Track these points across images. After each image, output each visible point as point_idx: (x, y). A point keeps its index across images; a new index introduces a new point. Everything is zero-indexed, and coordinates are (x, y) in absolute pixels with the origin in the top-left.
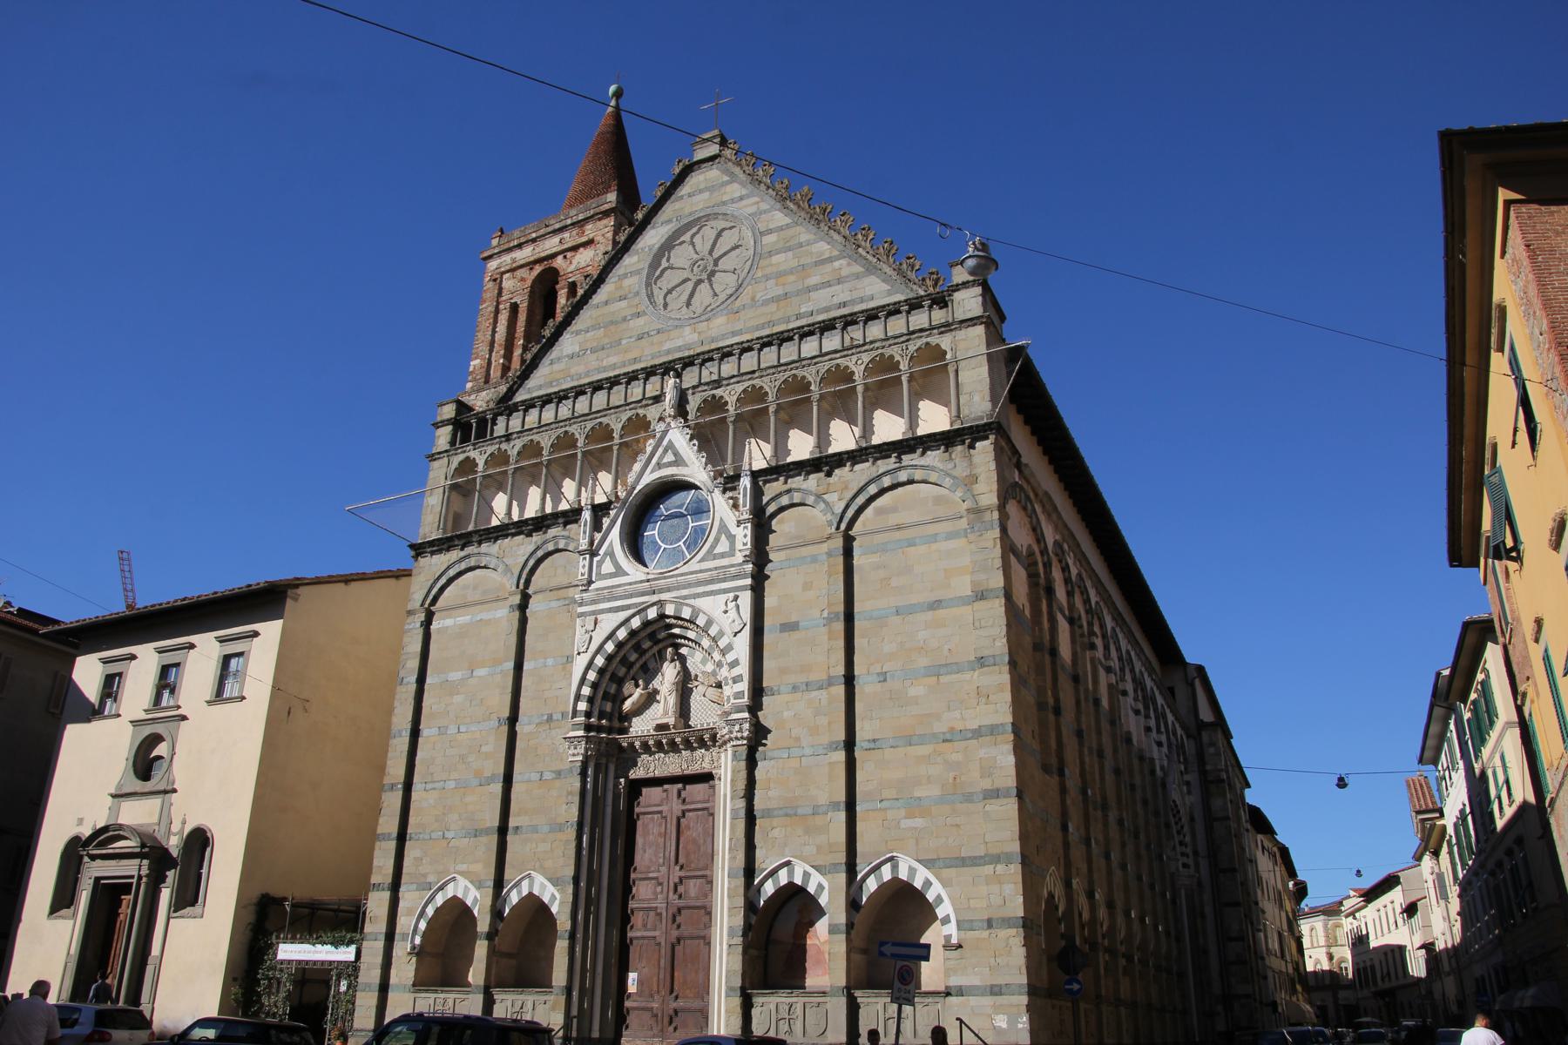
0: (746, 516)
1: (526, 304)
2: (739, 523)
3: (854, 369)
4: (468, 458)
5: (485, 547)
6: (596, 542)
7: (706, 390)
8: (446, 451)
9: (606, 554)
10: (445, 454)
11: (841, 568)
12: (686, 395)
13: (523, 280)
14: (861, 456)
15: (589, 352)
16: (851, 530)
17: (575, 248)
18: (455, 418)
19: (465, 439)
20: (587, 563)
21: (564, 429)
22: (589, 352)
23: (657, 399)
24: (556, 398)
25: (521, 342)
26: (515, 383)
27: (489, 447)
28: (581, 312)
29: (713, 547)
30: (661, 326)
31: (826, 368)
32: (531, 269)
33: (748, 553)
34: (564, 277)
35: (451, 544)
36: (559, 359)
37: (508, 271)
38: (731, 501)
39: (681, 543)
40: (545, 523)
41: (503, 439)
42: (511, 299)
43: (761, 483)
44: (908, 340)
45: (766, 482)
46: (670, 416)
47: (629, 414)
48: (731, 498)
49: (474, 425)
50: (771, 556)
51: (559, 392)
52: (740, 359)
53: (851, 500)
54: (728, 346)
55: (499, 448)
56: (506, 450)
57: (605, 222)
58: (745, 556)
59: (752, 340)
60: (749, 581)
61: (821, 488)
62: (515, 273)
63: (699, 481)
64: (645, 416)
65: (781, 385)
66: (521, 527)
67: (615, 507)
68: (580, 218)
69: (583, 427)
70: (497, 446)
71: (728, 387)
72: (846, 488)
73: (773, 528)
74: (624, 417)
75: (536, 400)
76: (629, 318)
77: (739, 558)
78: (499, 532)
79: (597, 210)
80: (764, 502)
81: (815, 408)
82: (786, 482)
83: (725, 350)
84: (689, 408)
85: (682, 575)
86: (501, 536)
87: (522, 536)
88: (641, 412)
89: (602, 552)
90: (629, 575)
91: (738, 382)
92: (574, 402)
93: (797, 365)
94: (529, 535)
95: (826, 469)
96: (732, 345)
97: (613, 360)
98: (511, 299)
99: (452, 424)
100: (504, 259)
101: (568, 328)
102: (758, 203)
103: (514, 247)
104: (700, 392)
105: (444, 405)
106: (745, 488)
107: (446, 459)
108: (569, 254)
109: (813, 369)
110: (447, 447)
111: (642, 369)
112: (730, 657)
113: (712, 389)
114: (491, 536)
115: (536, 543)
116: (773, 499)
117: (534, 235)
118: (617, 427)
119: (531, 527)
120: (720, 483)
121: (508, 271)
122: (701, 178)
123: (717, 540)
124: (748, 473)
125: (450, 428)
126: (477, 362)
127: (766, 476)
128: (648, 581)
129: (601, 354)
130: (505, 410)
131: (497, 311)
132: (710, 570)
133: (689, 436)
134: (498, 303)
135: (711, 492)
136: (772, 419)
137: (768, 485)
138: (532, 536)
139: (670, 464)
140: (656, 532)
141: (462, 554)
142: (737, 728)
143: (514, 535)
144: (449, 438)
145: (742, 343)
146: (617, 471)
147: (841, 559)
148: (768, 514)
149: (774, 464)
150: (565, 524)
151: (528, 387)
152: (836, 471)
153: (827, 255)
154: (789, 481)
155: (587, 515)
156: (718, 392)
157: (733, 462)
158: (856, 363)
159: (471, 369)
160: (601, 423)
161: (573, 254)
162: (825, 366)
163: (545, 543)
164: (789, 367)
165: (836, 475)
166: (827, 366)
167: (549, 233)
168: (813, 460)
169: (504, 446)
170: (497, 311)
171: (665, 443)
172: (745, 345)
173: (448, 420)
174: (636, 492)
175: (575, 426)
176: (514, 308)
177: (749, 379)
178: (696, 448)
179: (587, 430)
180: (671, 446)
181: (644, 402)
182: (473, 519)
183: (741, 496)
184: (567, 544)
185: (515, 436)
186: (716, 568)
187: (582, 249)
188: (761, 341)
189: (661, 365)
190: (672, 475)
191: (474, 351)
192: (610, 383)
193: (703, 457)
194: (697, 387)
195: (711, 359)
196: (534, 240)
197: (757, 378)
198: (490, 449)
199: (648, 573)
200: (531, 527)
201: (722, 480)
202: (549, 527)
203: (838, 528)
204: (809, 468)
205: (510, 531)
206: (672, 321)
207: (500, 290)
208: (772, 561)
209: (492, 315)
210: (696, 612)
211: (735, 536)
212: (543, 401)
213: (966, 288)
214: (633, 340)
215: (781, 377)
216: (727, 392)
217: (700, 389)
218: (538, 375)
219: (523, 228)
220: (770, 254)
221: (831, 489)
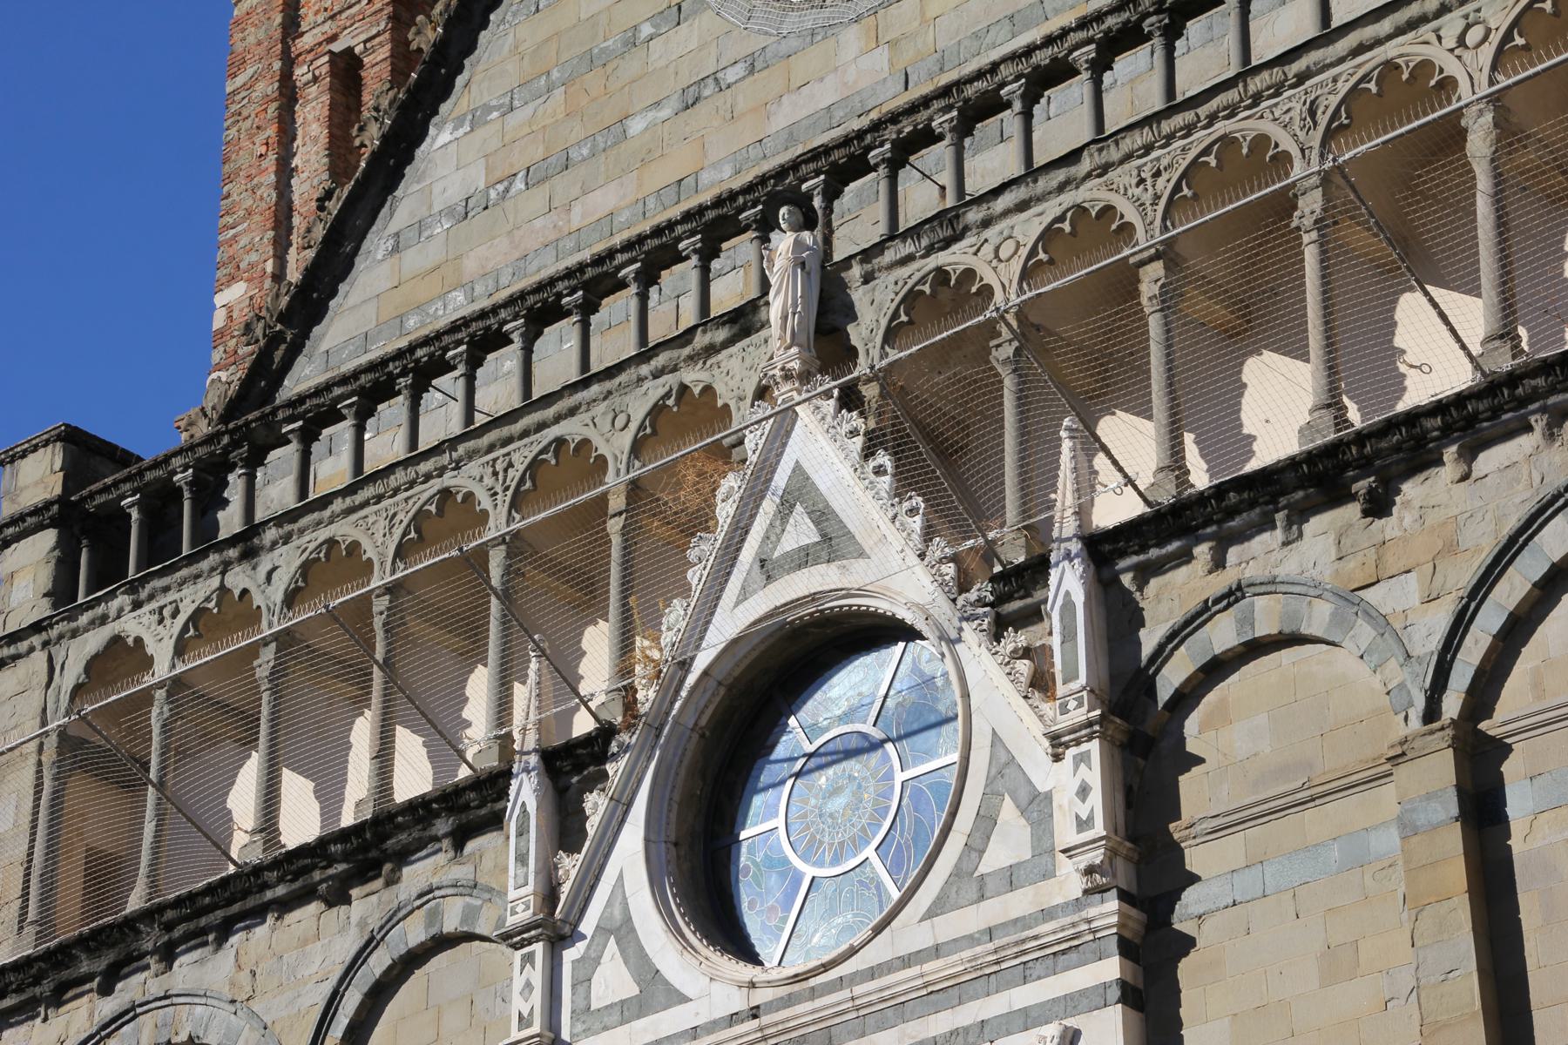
0: (1079, 715)
1: (384, 52)
2: (1058, 744)
3: (1452, 67)
5: (188, 970)
6: (566, 889)
7: (909, 259)
8: (37, 627)
9: (602, 930)
10: (36, 640)
11: (1456, 873)
12: (843, 286)
14: (1495, 412)
15: (519, 184)
16: (1488, 714)
18: (62, 500)
19: (108, 574)
20: (537, 975)
21: (436, 485)
22: (519, 184)
23: (745, 321)
24: (403, 374)
26: (274, 340)
27: (187, 591)
28: (484, 36)
29: (976, 847)
30: (757, 43)
31: (1343, 88)
33: (1096, 856)
35: (65, 974)
36: (421, 226)
38: (1024, 667)
39: (869, 851)
40: (390, 843)
41: (233, 553)
42: (333, 38)
43: (1126, 579)
45: (1145, 573)
46: (788, 376)
47: (654, 391)
48: (1027, 653)
49: (135, 514)
50: (1195, 859)
51: (412, 348)
52: (1027, 116)
53: (1473, 594)
54: (979, 75)
55: (223, 590)
56: (245, 592)
58: (1090, 871)
59: (1065, 32)
60: (1111, 968)
61: (1351, 564)
63: (911, 605)
64: (708, 390)
65: (1177, 188)
66: (307, 870)
67: (625, 749)
69: (500, 466)
70: (215, 582)
71: (988, 233)
72: (1451, 548)
73: (1191, 747)
74: (638, 406)
75: (337, 391)
76: (647, 30)
77: (1069, 881)
78: (230, 902)
80: (1147, 650)
81: (1311, 255)
82: (1219, 563)
83: (970, 91)
84: (856, 334)
85: (872, 973)
86: (242, 916)
87: (314, 907)
88: (693, 376)
89: (587, 926)
90: (684, 999)
91: (1022, 206)
92: (470, 379)
93: (1231, 96)
94: (338, 897)
95: (1361, 486)
96: (994, 68)
97: (604, 200)
98: (333, 38)
101: (444, 108)
104: (891, 266)
105: (24, 455)
106: (1068, 606)
107: (39, 659)
109: (1293, 102)
110: (44, 609)
111: (687, 216)
113: (930, 250)
114: (203, 921)
115: (362, 923)
116: (1176, 637)
118: (614, 445)
119: (341, 867)
120: (980, 602)
123: (986, 821)
124: (1075, 546)
125: (49, 537)
127: (1143, 549)
128: (755, 1013)
129: (563, 186)
131: (288, 95)
132: (971, 940)
133: (859, 441)
134: (289, 62)
135: (952, 642)
136: (1155, 325)
137: (1154, 583)
138: (347, 901)
139: (804, 558)
140: (779, 822)
141: (108, 1007)
143: (285, 906)
145: (1029, 51)
146: (626, 611)
147: (1453, 840)
148: (1164, 693)
149: (1166, 497)
150: (460, 838)
151: (324, 347)
152: (1407, 487)
154: (1233, 554)
155: (526, 792)
156: (955, 258)
157: (1025, 512)
158: (1461, 41)
159: (219, 320)
160: (560, 442)
162: (1331, 88)
163: (393, 920)
164: (1203, 111)
165: (1407, 504)
166: (1347, 76)
168: (1310, 457)
169: (238, 579)
170: (288, 95)
171: (781, 479)
172: (1042, 57)
173: (36, 511)
174: (691, 680)
175: (473, 468)
176: (347, 69)
177: (1061, 188)
178: (885, 482)
179: (514, 475)
180: (801, 491)
181: (700, 340)
182: (143, 869)
183: (1056, 641)
184: (470, 914)
185: (271, 534)
186: (990, 933)
188: (1096, 31)
189: (749, 189)
190: (813, 597)
191: (220, 256)
192: (586, 286)
193: (912, 512)
194: (878, 248)
195: (927, 137)
197: (1088, 176)
198: (192, 596)
199: (752, 985)
200: (341, 867)
201: (982, 589)
202: (403, 857)
203: (1432, 713)
204: (1300, 494)
205: (269, 895)
208: (1193, 879)
211: (1048, 797)
212: (361, 392)
214: (666, 112)
215: (1177, 156)
216: (987, 250)
217: (889, 256)
218: (353, 300)
221: (1393, 563)
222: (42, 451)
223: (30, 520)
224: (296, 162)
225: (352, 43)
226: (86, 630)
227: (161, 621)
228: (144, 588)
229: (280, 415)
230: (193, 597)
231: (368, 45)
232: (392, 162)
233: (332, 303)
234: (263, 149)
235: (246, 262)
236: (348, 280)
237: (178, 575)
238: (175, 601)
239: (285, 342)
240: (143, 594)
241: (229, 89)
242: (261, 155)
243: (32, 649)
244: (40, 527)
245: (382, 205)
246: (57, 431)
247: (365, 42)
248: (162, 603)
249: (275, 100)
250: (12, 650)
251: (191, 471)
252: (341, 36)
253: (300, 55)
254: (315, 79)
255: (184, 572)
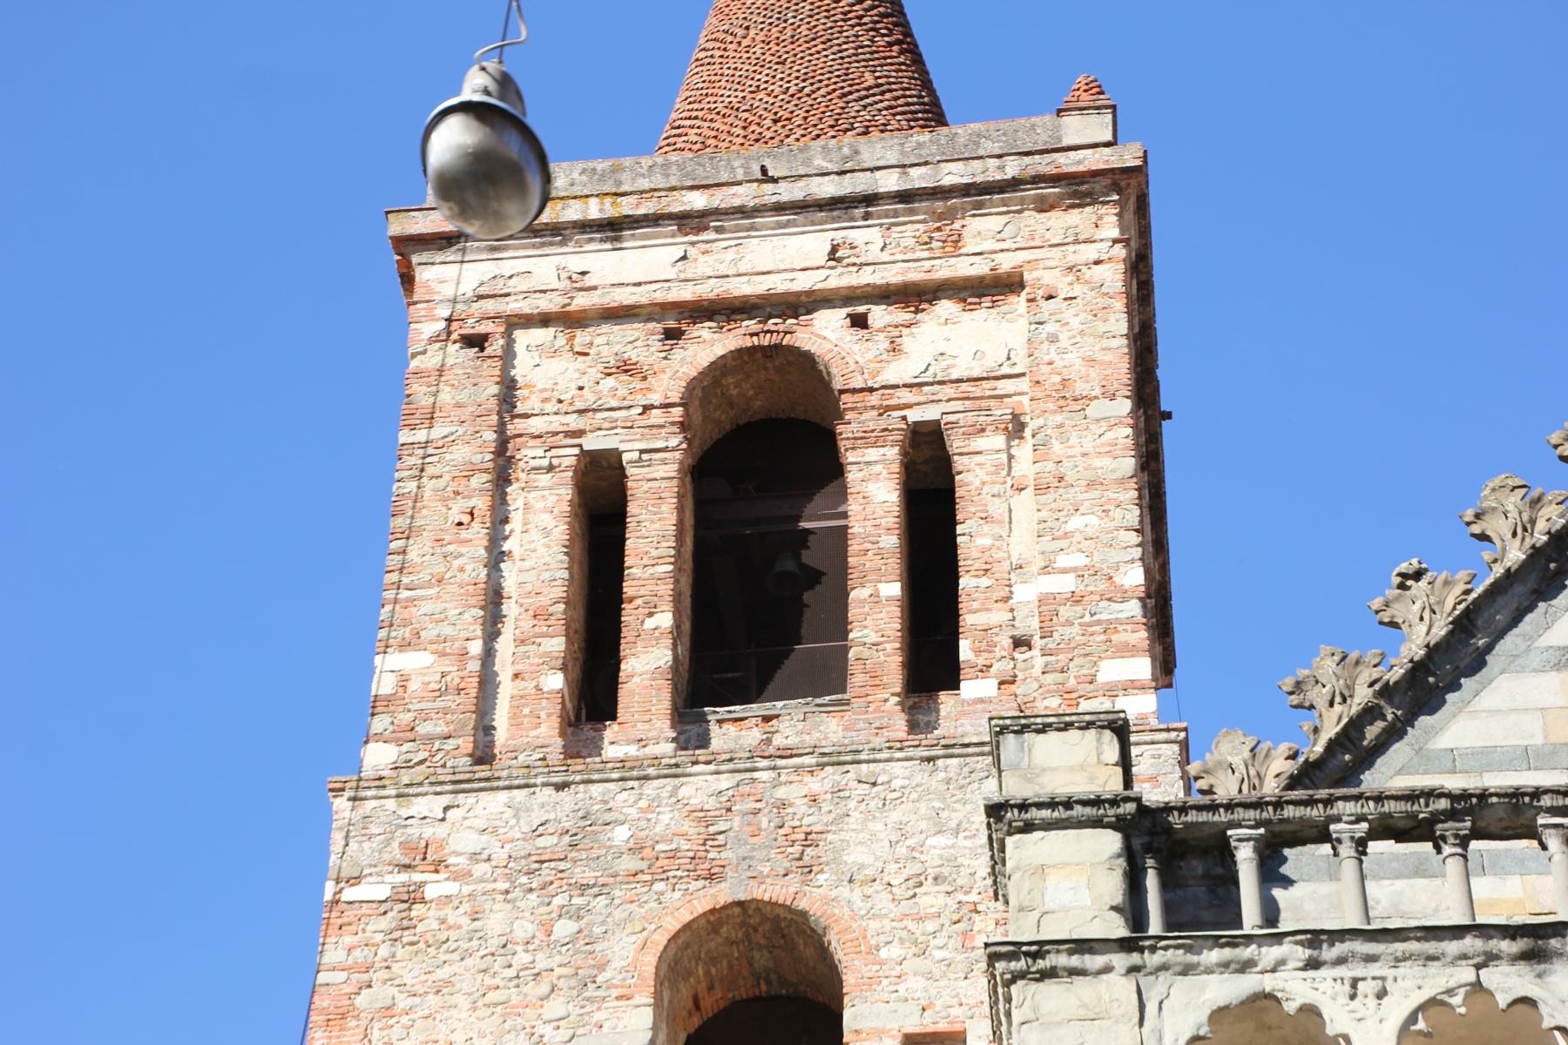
4: (1265, 1000)
10: (1120, 960)
13: (625, 368)
17: (915, 296)
25: (665, 619)
27: (1405, 969)
32: (672, 335)
34: (874, 399)
37: (545, 320)
41: (1506, 946)
55: (1477, 986)
57: (1077, 219)
62: (582, 337)
68: (947, 181)
70: (1466, 974)
79: (1043, 165)
98: (579, 433)
99: (1119, 825)
100: (521, 265)
103: (585, 226)
105: (1043, 729)
108: (879, 315)
117: (697, 201)
121: (545, 320)
126: (415, 662)
130: (1452, 815)
144: (1113, 886)
151: (1444, 741)
159: (384, 685)
161: (902, 316)
167: (779, 208)
173: (1096, 802)
187: (946, 307)
196: (690, 222)
207: (509, 388)
209: (480, 480)
219: (601, 165)
222: (1073, 734)
223: (1078, 810)
224: (506, 547)
225: (622, 447)
226: (1209, 971)
227: (1353, 997)
228: (1332, 945)
229: (1546, 801)
230: (1420, 982)
231: (645, 456)
232: (1552, 566)
233: (1450, 697)
234: (466, 519)
235: (435, 632)
236: (1477, 677)
237: (1399, 947)
238: (1383, 979)
239: (1386, 720)
240: (1329, 953)
241: (402, 440)
242: (460, 524)
243: (1108, 969)
244: (1097, 823)
245: (1531, 608)
246: (1111, 717)
247: (642, 452)
248: (1358, 973)
249: (486, 471)
250: (1075, 961)
251: (1364, 826)
252: (590, 435)
253: (520, 436)
254: (551, 468)
255: (1413, 946)
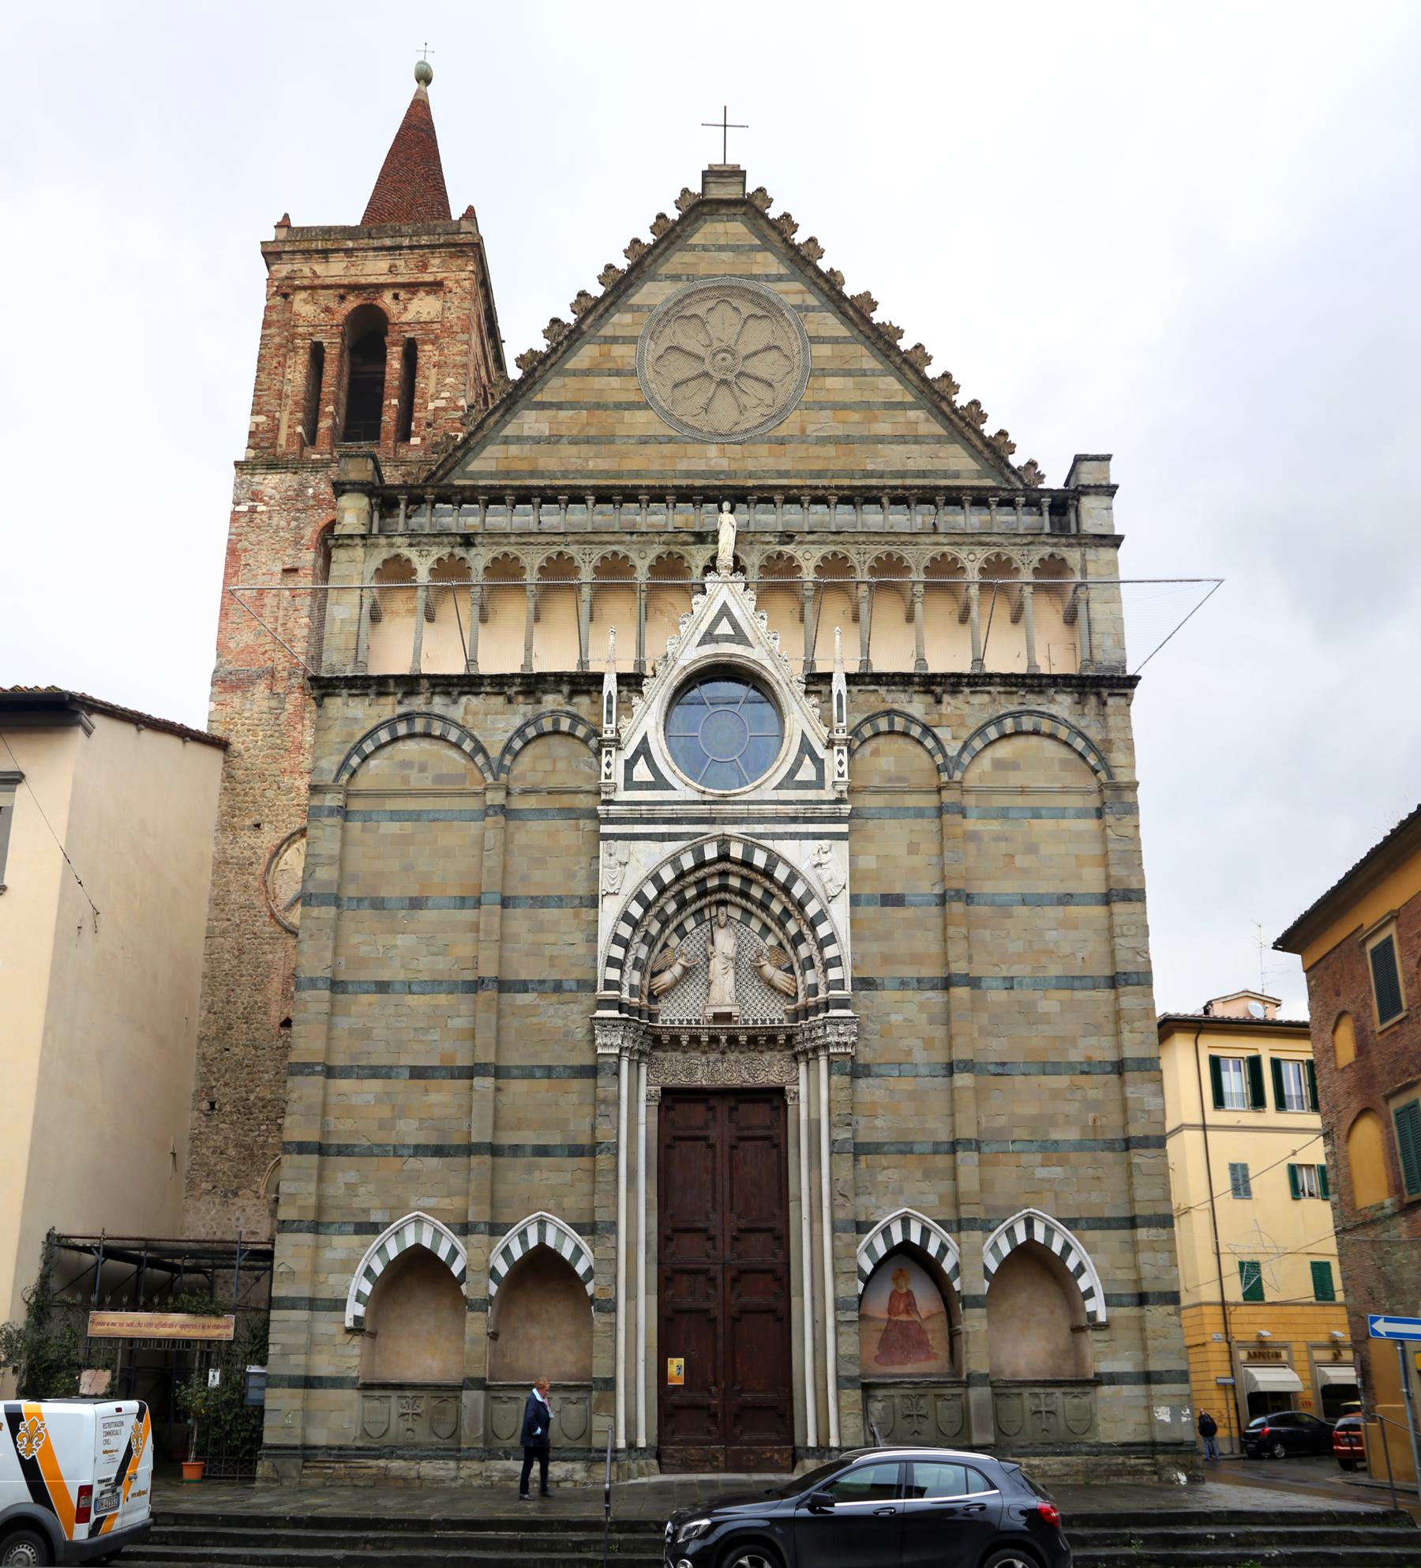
30: (674, 433)
44: (1031, 543)
102: (802, 292)
112: (823, 930)
122: (720, 227)
142: (842, 1029)
153: (898, 399)
206: (689, 430)
210: (774, 858)
213: (1097, 494)
220: (824, 373)
